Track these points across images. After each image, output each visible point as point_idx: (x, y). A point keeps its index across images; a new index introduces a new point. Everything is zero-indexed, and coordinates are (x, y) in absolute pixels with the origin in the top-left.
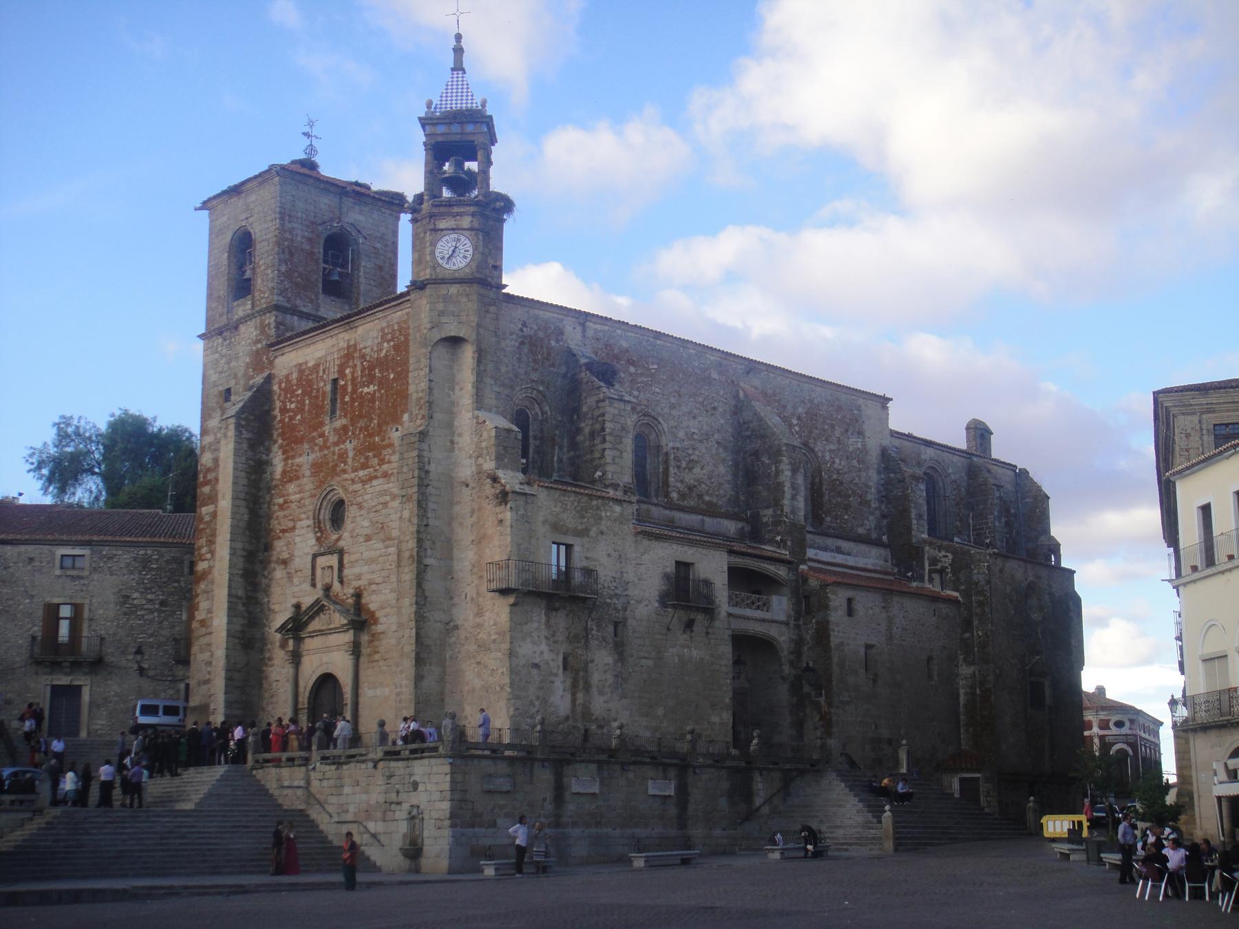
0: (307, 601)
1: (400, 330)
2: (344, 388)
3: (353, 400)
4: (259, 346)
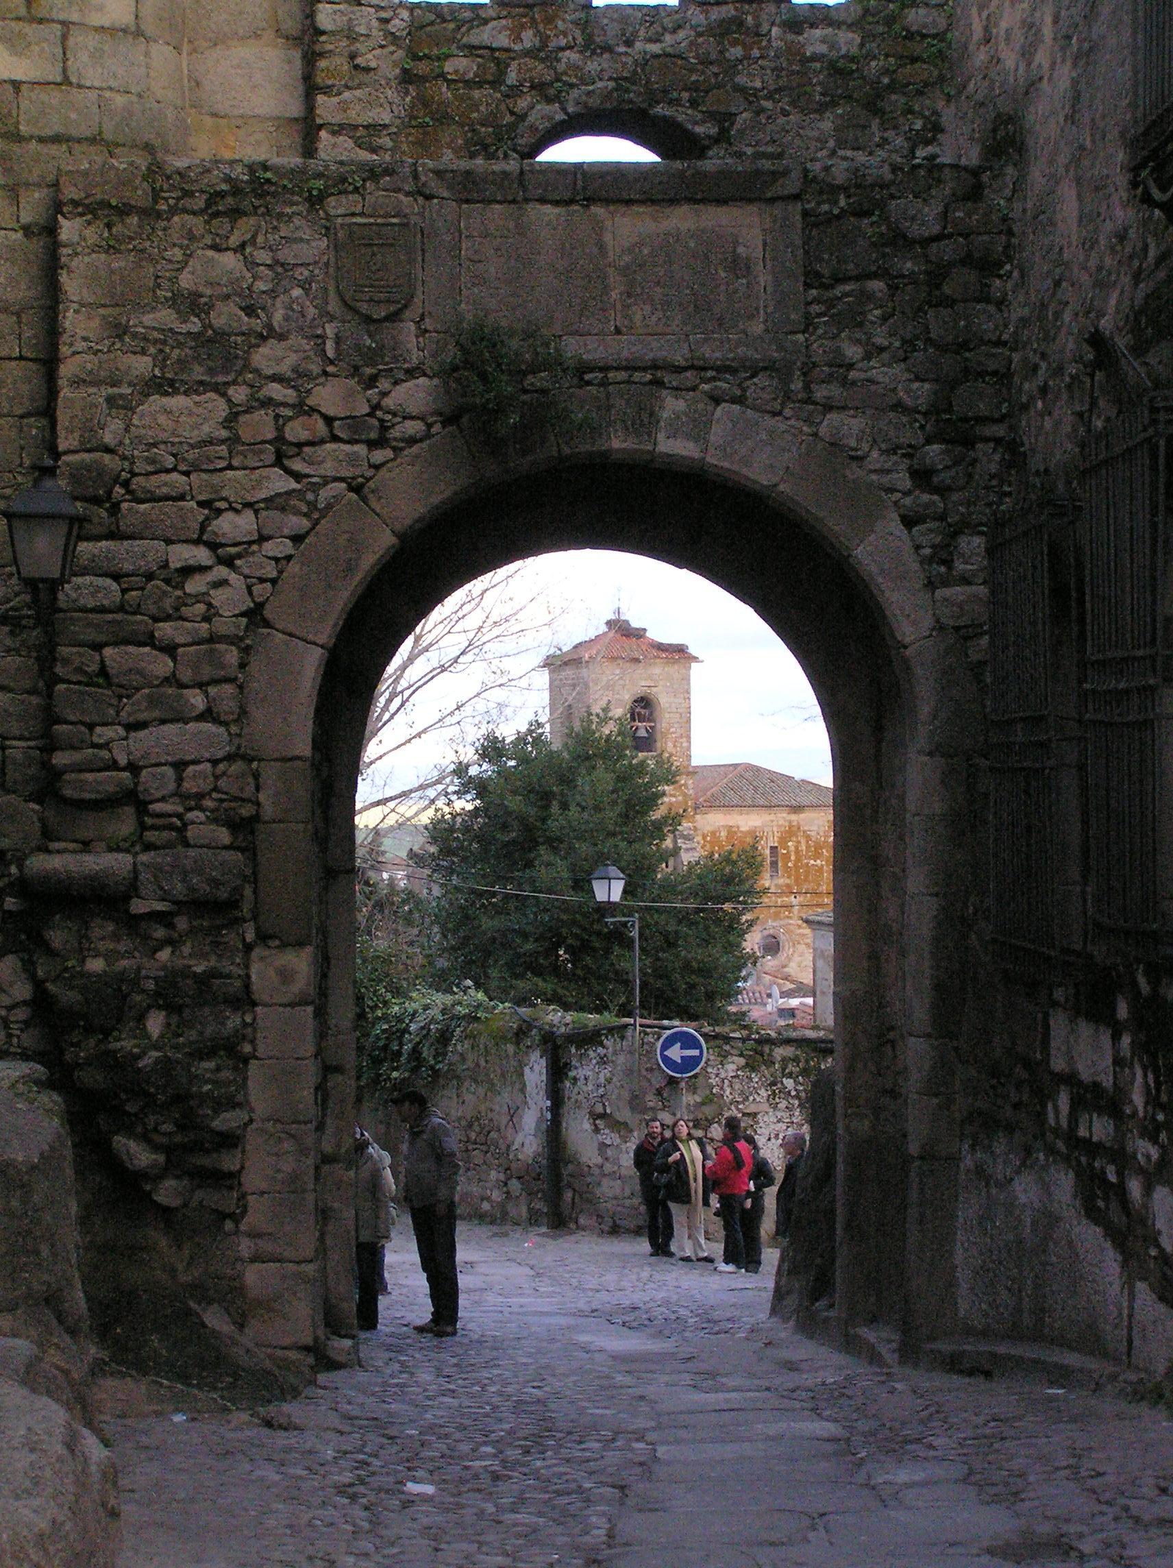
2: (787, 857)
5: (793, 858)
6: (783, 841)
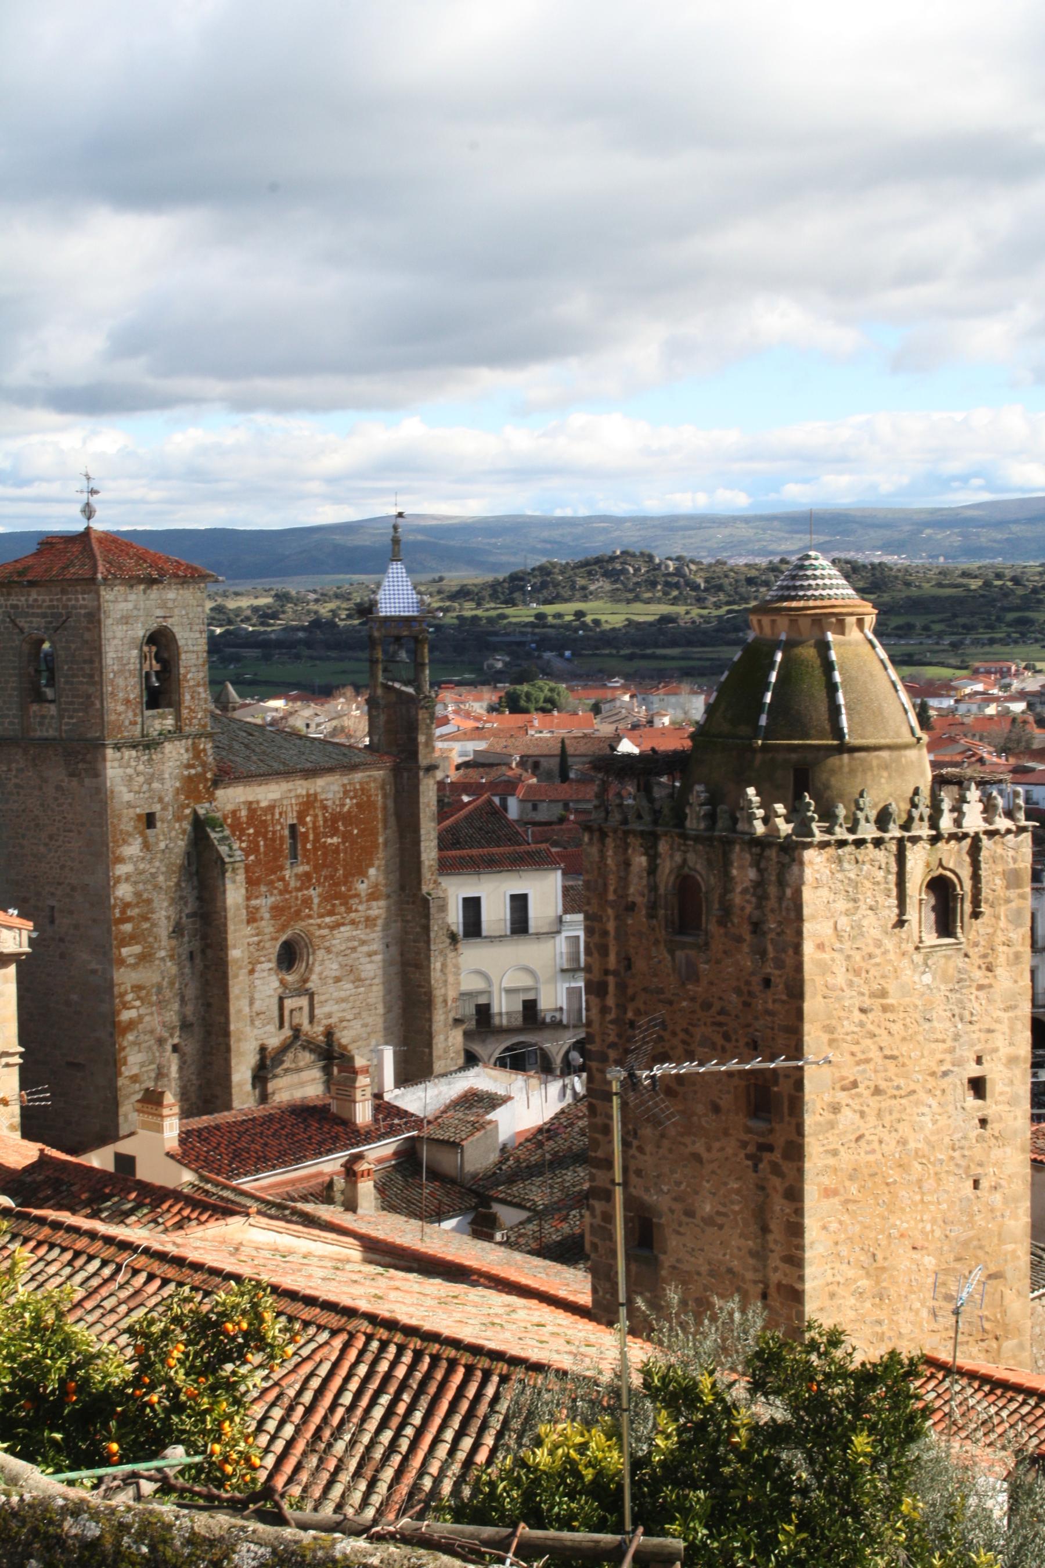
0: (274, 1041)
1: (362, 789)
2: (305, 835)
3: (315, 849)
4: (193, 771)
5: (311, 837)
6: (301, 816)
